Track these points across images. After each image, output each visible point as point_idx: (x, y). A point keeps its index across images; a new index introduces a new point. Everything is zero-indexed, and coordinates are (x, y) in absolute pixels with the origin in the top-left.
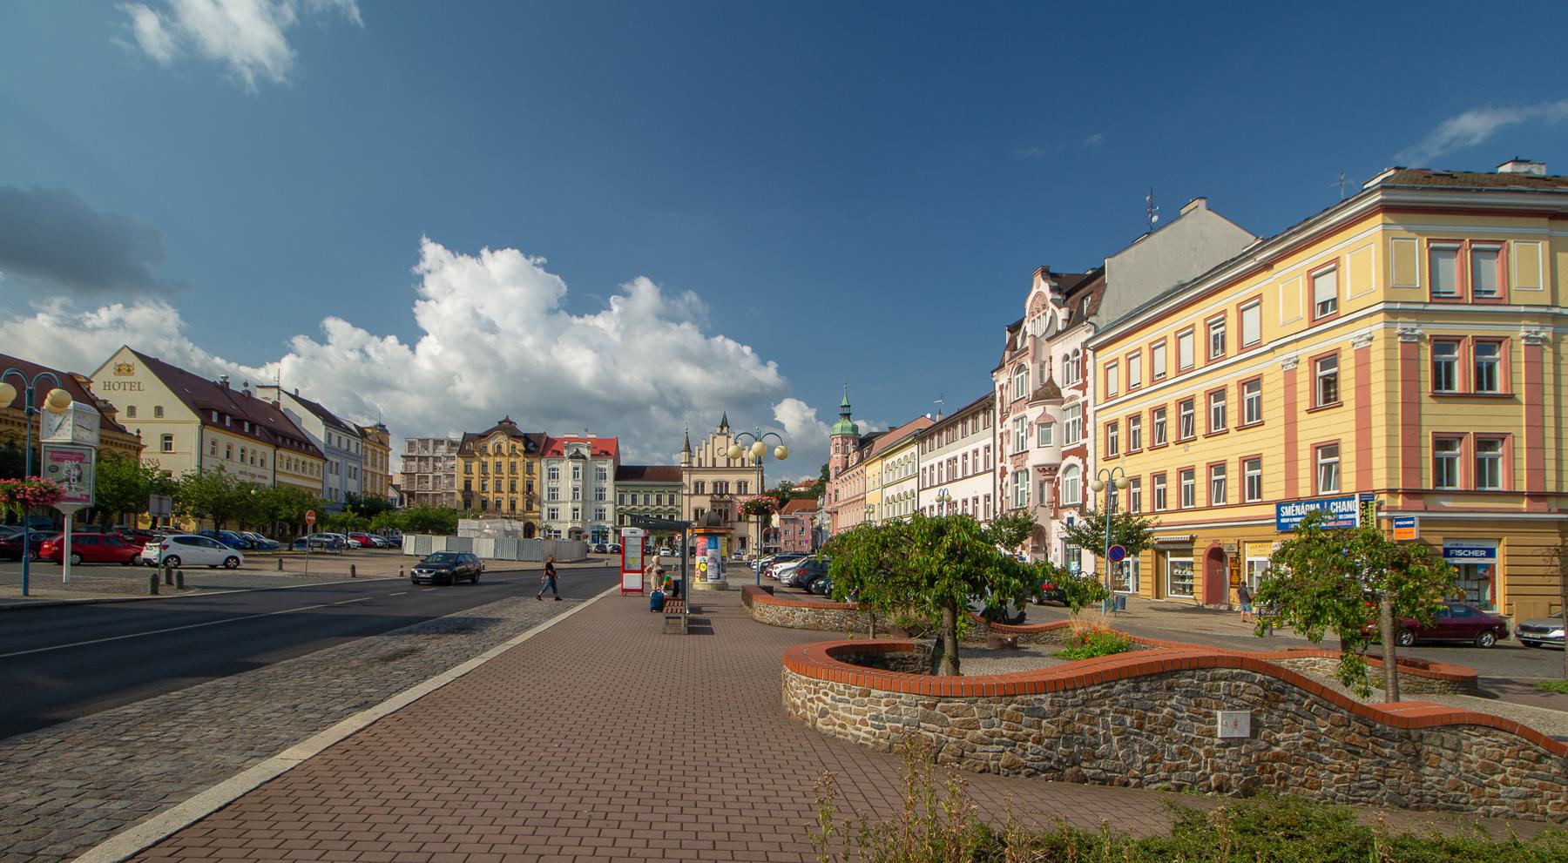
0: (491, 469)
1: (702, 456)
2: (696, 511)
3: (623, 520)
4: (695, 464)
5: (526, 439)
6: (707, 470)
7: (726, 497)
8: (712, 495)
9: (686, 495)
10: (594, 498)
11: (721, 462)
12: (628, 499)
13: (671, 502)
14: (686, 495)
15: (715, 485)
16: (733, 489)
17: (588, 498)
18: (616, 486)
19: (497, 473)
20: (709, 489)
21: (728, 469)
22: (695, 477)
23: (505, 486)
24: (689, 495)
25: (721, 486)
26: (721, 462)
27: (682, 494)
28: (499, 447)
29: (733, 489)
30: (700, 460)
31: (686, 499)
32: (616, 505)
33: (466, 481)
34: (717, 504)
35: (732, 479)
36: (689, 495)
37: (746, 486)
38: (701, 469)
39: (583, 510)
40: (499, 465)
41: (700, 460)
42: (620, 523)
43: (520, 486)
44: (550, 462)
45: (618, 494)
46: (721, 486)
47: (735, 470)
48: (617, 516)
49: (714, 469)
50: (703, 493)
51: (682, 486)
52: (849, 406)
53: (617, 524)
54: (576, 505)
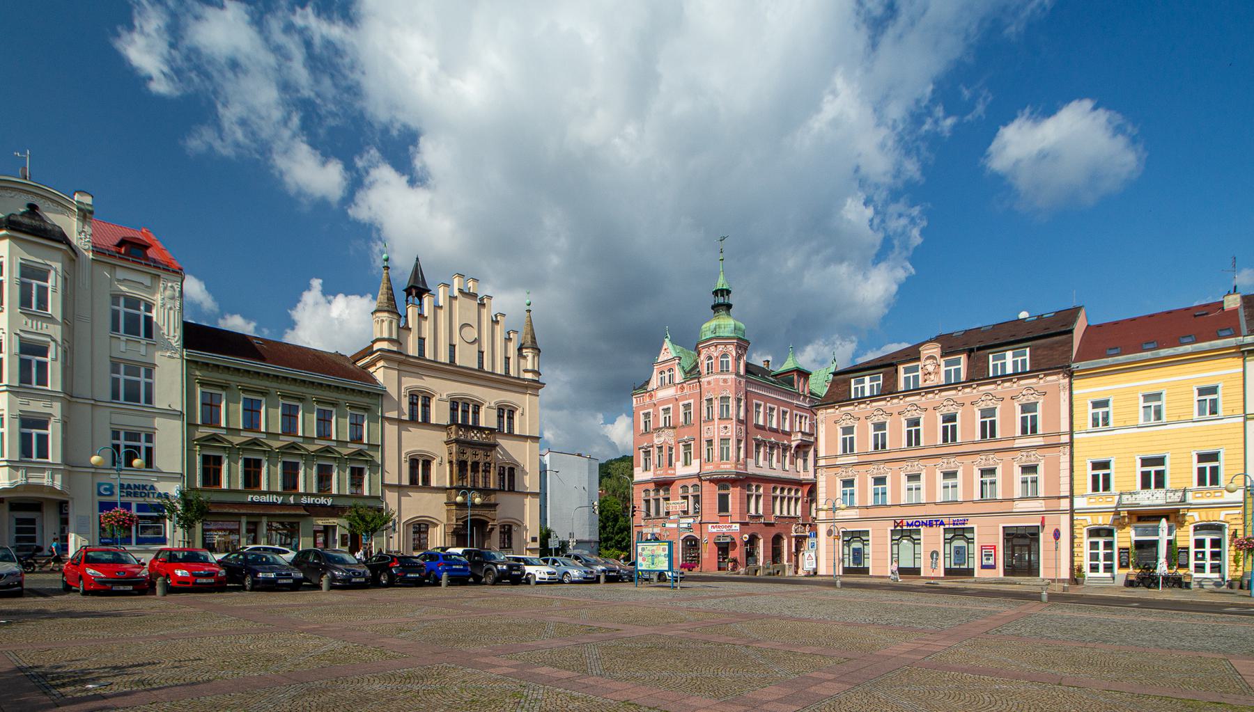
1: (427, 333)
2: (414, 463)
4: (412, 350)
6: (436, 369)
9: (391, 420)
10: (107, 395)
12: (231, 413)
14: (391, 420)
15: (454, 405)
17: (83, 388)
18: (191, 363)
22: (410, 382)
24: (399, 421)
25: (465, 412)
27: (383, 417)
30: (421, 341)
31: (392, 430)
32: (191, 425)
34: (469, 452)
35: (490, 397)
36: (399, 421)
38: (421, 365)
39: (65, 424)
41: (421, 341)
42: (206, 481)
45: (199, 390)
46: (465, 412)
48: (198, 459)
49: (451, 370)
51: (379, 395)
52: (728, 292)
53: (199, 485)
54: (37, 407)
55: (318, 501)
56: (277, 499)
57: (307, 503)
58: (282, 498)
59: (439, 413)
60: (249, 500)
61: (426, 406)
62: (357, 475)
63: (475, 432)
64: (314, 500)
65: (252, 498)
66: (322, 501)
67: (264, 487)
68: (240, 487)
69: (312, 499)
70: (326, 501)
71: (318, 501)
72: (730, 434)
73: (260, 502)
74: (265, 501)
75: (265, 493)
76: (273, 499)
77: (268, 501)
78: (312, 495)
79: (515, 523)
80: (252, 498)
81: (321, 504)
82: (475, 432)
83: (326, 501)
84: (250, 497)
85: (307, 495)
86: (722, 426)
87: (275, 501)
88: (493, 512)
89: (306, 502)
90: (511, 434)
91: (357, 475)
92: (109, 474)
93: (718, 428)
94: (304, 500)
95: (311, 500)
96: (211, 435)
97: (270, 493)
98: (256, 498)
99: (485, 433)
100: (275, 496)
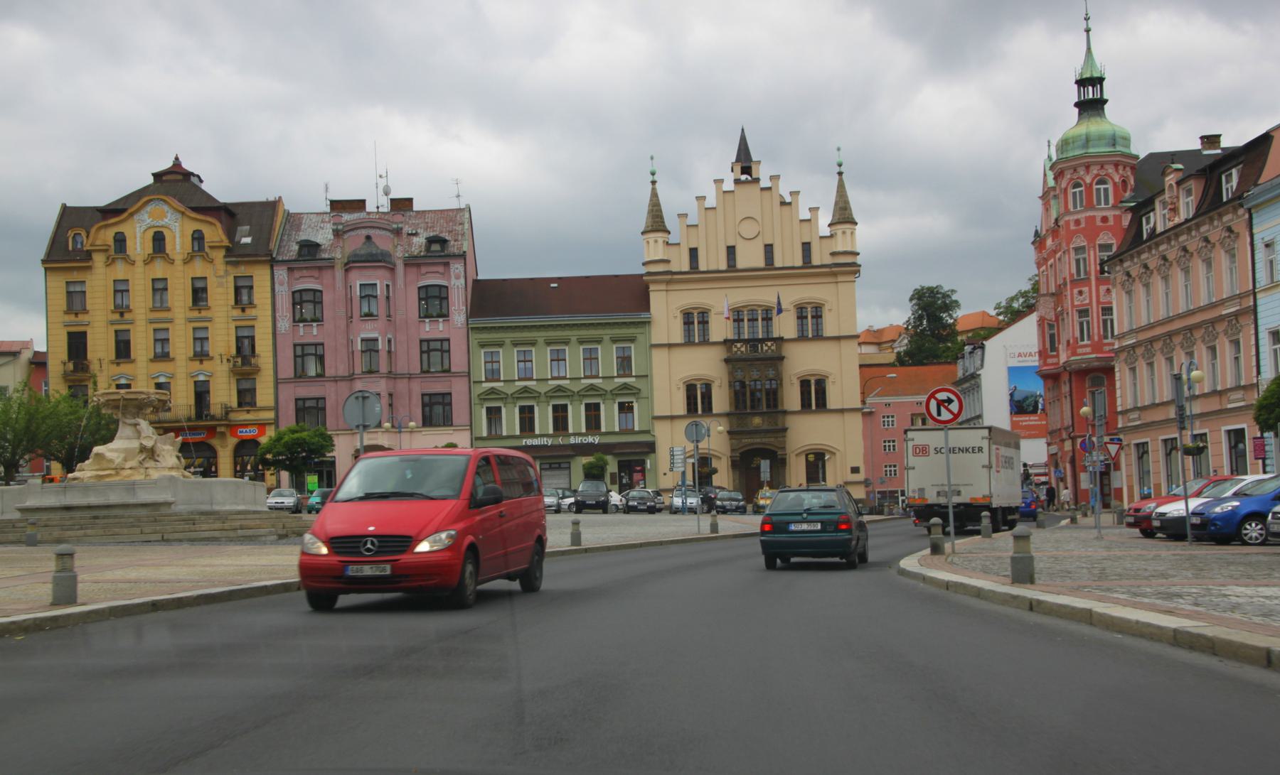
0: (140, 299)
2: (690, 389)
3: (565, 418)
5: (228, 214)
6: (714, 277)
7: (767, 347)
8: (727, 343)
11: (750, 257)
13: (625, 363)
15: (737, 316)
16: (785, 326)
19: (154, 309)
20: (720, 329)
21: (770, 268)
23: (181, 345)
26: (750, 257)
28: (159, 240)
29: (785, 326)
33: (70, 335)
37: (818, 316)
40: (159, 288)
43: (222, 341)
44: (297, 274)
47: (789, 274)
49: (732, 271)
50: (705, 342)
55: (585, 440)
57: (575, 444)
59: (720, 329)
60: (524, 444)
61: (704, 322)
62: (625, 408)
63: (739, 352)
64: (581, 440)
65: (526, 442)
66: (590, 439)
67: (537, 432)
68: (518, 433)
69: (580, 438)
70: (594, 439)
71: (585, 440)
72: (1087, 301)
73: (532, 445)
75: (537, 436)
76: (544, 441)
78: (580, 434)
79: (827, 450)
81: (588, 443)
82: (739, 352)
83: (594, 439)
84: (524, 441)
85: (575, 435)
86: (1076, 291)
87: (546, 443)
88: (781, 439)
90: (818, 337)
91: (625, 408)
92: (421, 431)
93: (1072, 294)
94: (572, 440)
95: (578, 440)
96: (490, 390)
97: (542, 436)
98: (530, 442)
99: (766, 345)
100: (545, 439)
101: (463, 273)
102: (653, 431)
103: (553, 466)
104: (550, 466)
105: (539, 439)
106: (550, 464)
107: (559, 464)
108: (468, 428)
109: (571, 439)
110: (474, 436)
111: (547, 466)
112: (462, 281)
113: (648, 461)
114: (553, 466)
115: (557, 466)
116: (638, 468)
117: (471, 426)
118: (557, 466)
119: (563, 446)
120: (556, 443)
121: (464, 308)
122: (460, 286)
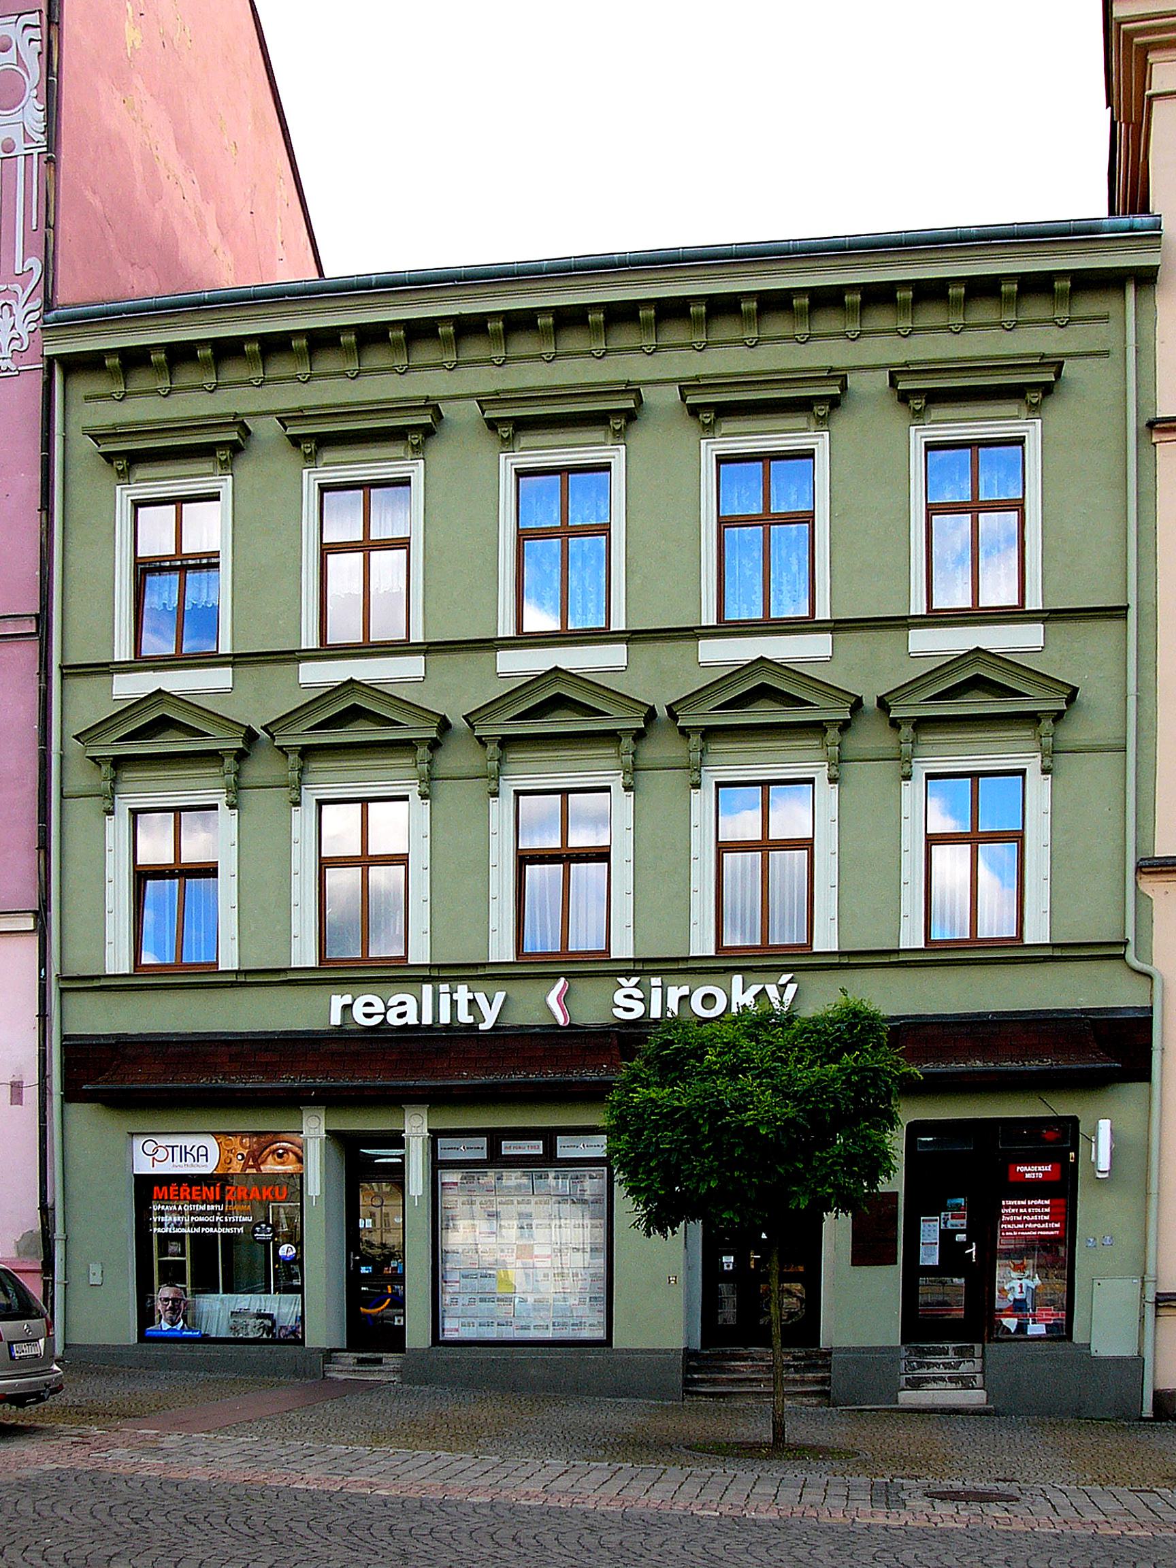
55: (709, 999)
56: (472, 1002)
58: (499, 997)
60: (336, 1019)
65: (347, 1008)
71: (709, 999)
74: (411, 1019)
77: (427, 1020)
80: (347, 1008)
84: (338, 1002)
87: (464, 1017)
89: (639, 1009)
100: (463, 994)
101: (35, 69)
102: (1144, 951)
103: (510, 1148)
104: (494, 1149)
105: (427, 989)
106: (495, 1137)
107: (548, 1136)
108: (29, 923)
109: (619, 998)
110: (55, 969)
111: (477, 1149)
112: (32, 114)
113: (1104, 1126)
114: (510, 1148)
115: (535, 1148)
116: (1032, 1172)
117: (41, 914)
118: (535, 1148)
119: (573, 1032)
120: (526, 1016)
121: (36, 264)
122: (19, 150)
